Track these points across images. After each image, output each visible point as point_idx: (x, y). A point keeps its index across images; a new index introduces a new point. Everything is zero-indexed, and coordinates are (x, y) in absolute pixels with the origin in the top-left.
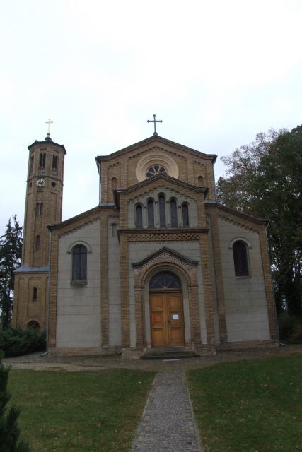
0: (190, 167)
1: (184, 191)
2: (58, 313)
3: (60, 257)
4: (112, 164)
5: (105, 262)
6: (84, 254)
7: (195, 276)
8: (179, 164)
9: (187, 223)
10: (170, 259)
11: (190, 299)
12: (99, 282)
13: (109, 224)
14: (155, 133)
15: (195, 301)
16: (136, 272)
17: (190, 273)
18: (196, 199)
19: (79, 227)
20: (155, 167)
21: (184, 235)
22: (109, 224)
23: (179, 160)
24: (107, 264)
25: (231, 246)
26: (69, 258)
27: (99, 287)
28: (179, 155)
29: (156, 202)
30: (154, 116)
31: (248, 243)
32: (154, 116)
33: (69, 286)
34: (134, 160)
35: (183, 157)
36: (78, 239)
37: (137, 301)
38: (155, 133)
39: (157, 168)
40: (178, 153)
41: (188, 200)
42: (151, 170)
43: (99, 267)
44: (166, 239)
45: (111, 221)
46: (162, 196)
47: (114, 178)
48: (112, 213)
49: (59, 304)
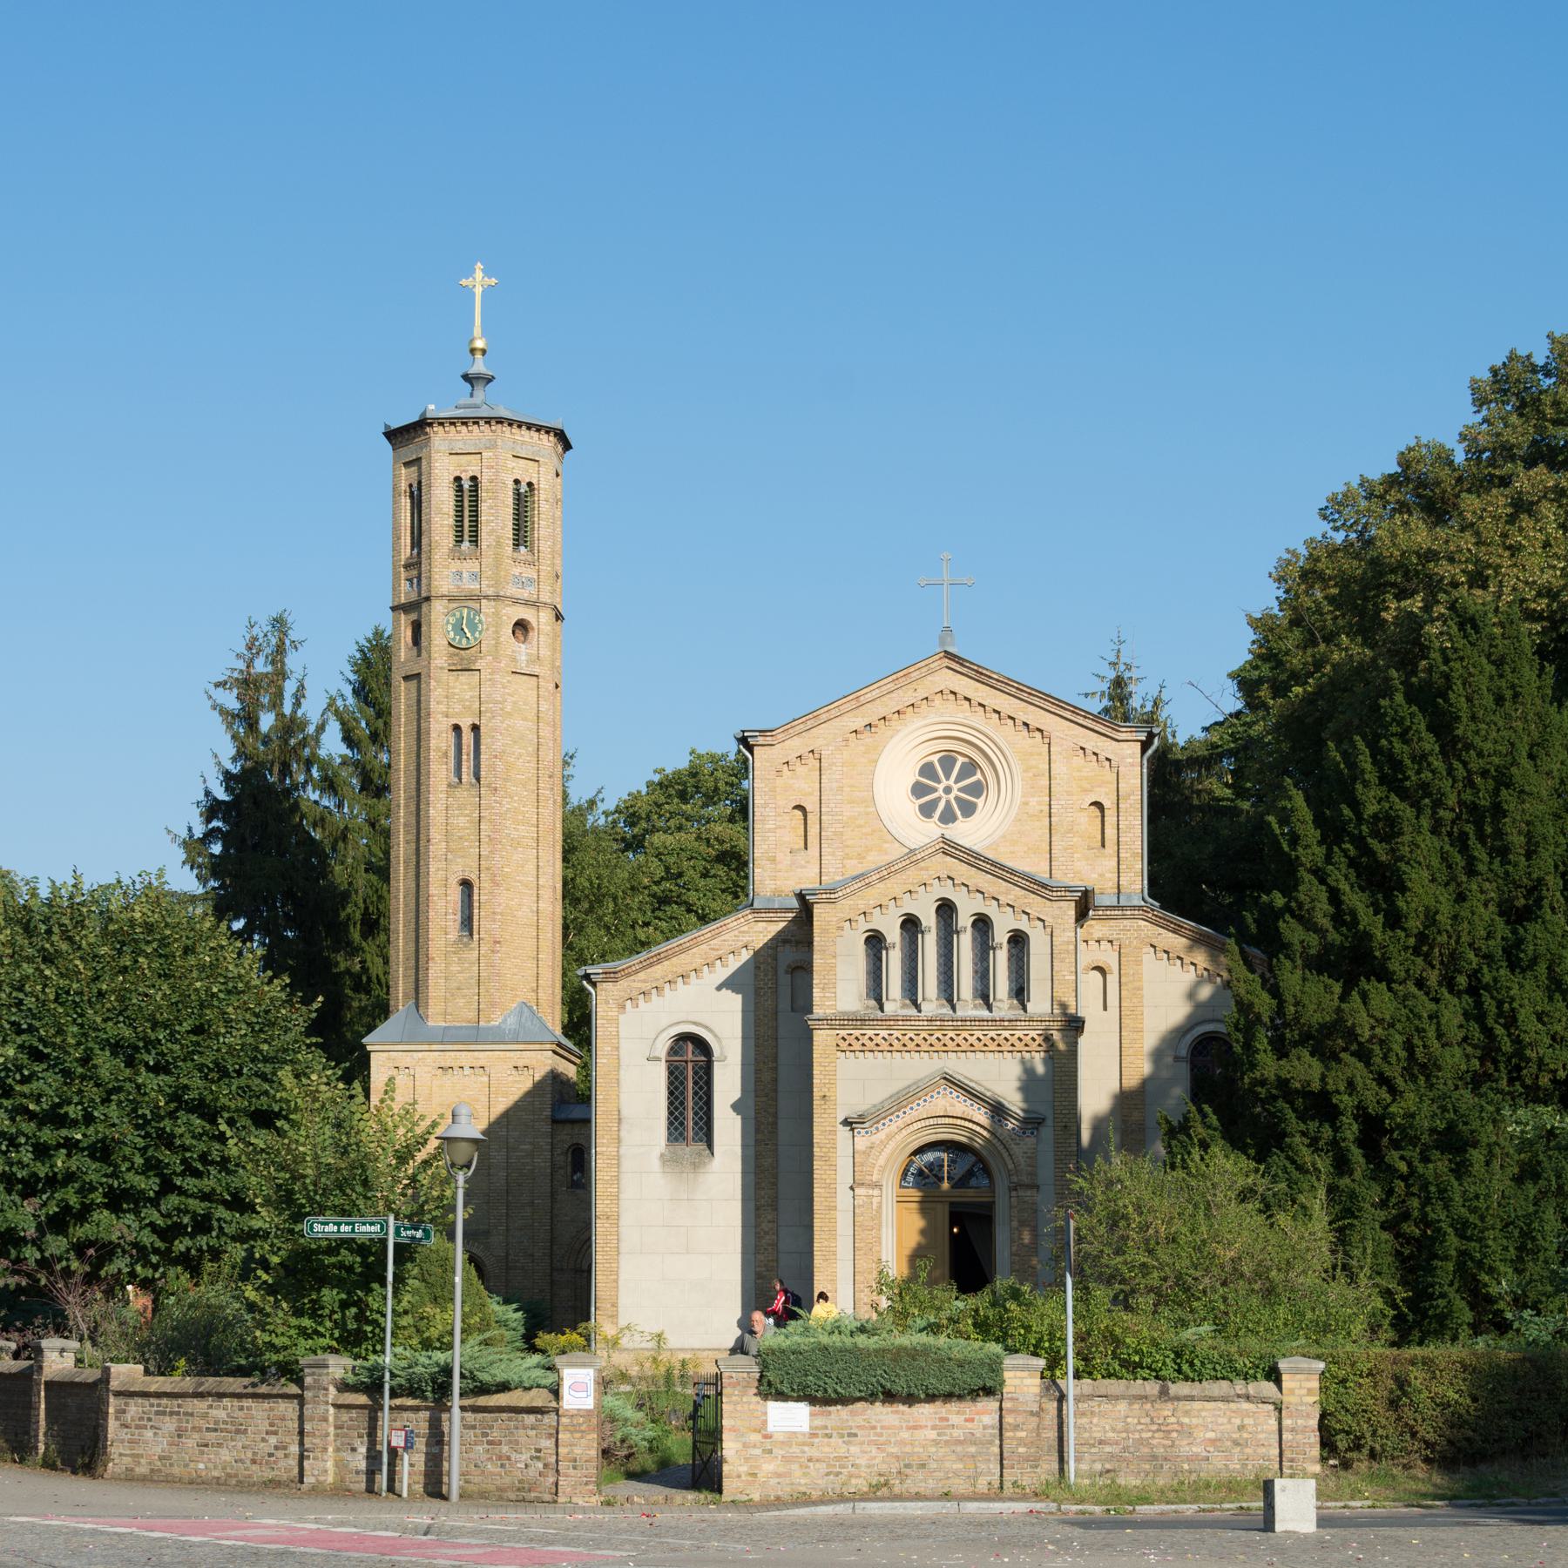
1: (1013, 894)
2: (624, 1247)
3: (624, 1075)
4: (792, 757)
9: (1020, 992)
22: (781, 971)
25: (1184, 1052)
28: (1026, 724)
33: (656, 1164)
34: (867, 737)
36: (682, 1017)
40: (1021, 717)
41: (1023, 925)
42: (927, 770)
46: (946, 909)
47: (799, 807)
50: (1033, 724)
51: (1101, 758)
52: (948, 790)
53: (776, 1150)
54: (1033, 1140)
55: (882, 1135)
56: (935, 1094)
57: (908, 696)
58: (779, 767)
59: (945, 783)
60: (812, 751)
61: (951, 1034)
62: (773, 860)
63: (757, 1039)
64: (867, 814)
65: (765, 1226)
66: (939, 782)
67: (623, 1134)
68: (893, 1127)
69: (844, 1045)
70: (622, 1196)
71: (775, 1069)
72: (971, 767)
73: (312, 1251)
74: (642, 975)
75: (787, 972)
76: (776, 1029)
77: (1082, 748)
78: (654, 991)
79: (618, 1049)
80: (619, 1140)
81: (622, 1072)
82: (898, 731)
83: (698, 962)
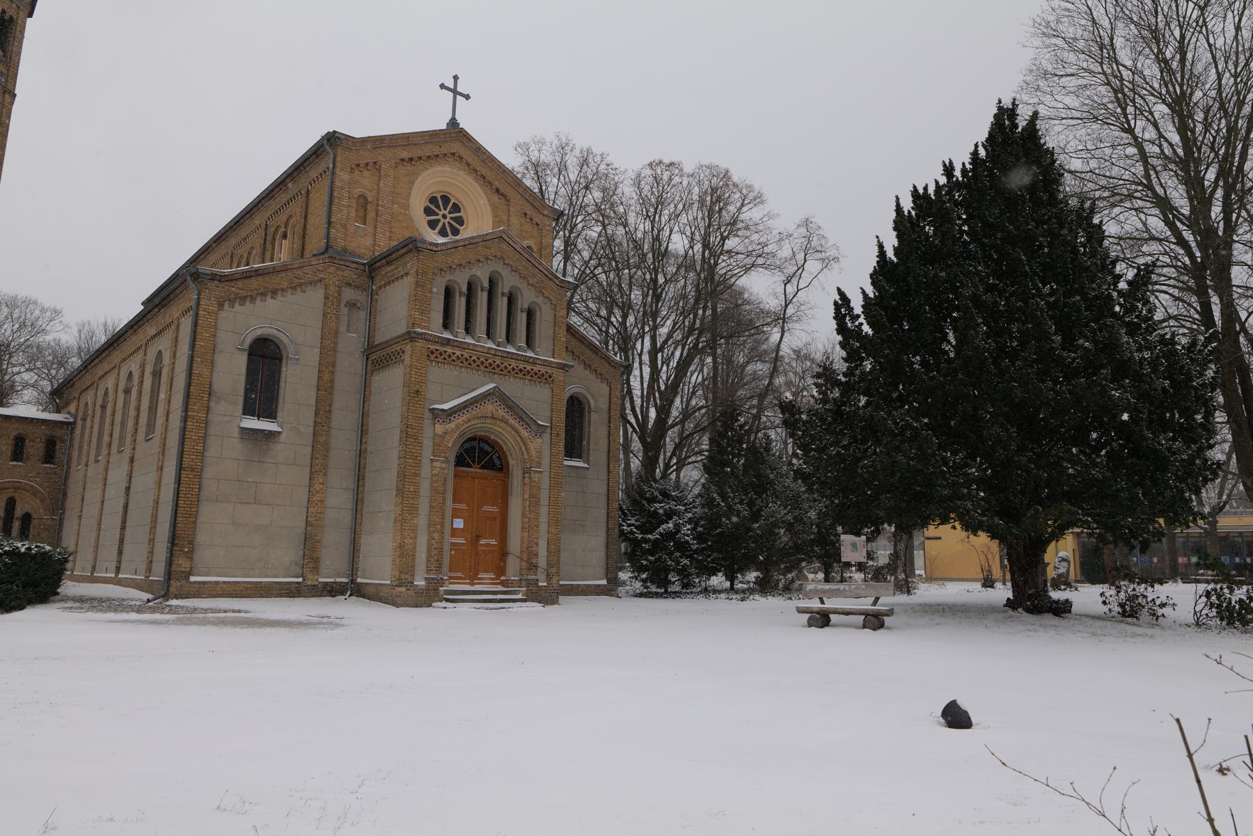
0: (515, 220)
4: (363, 163)
5: (325, 390)
6: (276, 359)
7: (540, 452)
8: (494, 209)
10: (501, 413)
11: (526, 496)
12: (311, 429)
13: (343, 302)
14: (453, 123)
15: (534, 501)
16: (439, 429)
17: (532, 446)
18: (554, 301)
19: (274, 293)
20: (442, 197)
21: (529, 368)
22: (342, 306)
23: (495, 198)
24: (331, 394)
26: (241, 361)
27: (310, 444)
28: (497, 190)
29: (503, 294)
30: (456, 78)
31: (592, 402)
32: (456, 78)
35: (503, 195)
37: (434, 490)
38: (453, 123)
39: (446, 199)
42: (433, 200)
43: (310, 396)
44: (497, 370)
45: (349, 294)
47: (363, 196)
48: (349, 274)
49: (208, 473)
50: (502, 190)
51: (534, 222)
52: (444, 217)
53: (329, 431)
54: (541, 441)
55: (453, 425)
56: (499, 403)
57: (436, 151)
58: (353, 166)
59: (446, 212)
60: (375, 163)
61: (498, 362)
62: (344, 226)
63: (322, 348)
64: (405, 215)
65: (317, 487)
66: (445, 209)
67: (212, 404)
68: (460, 420)
69: (432, 357)
70: (206, 454)
71: (333, 373)
72: (456, 208)
73: (839, 403)
74: (240, 284)
75: (346, 306)
76: (336, 343)
77: (525, 214)
78: (249, 298)
79: (214, 336)
80: (208, 408)
81: (216, 356)
82: (427, 169)
83: (285, 284)
